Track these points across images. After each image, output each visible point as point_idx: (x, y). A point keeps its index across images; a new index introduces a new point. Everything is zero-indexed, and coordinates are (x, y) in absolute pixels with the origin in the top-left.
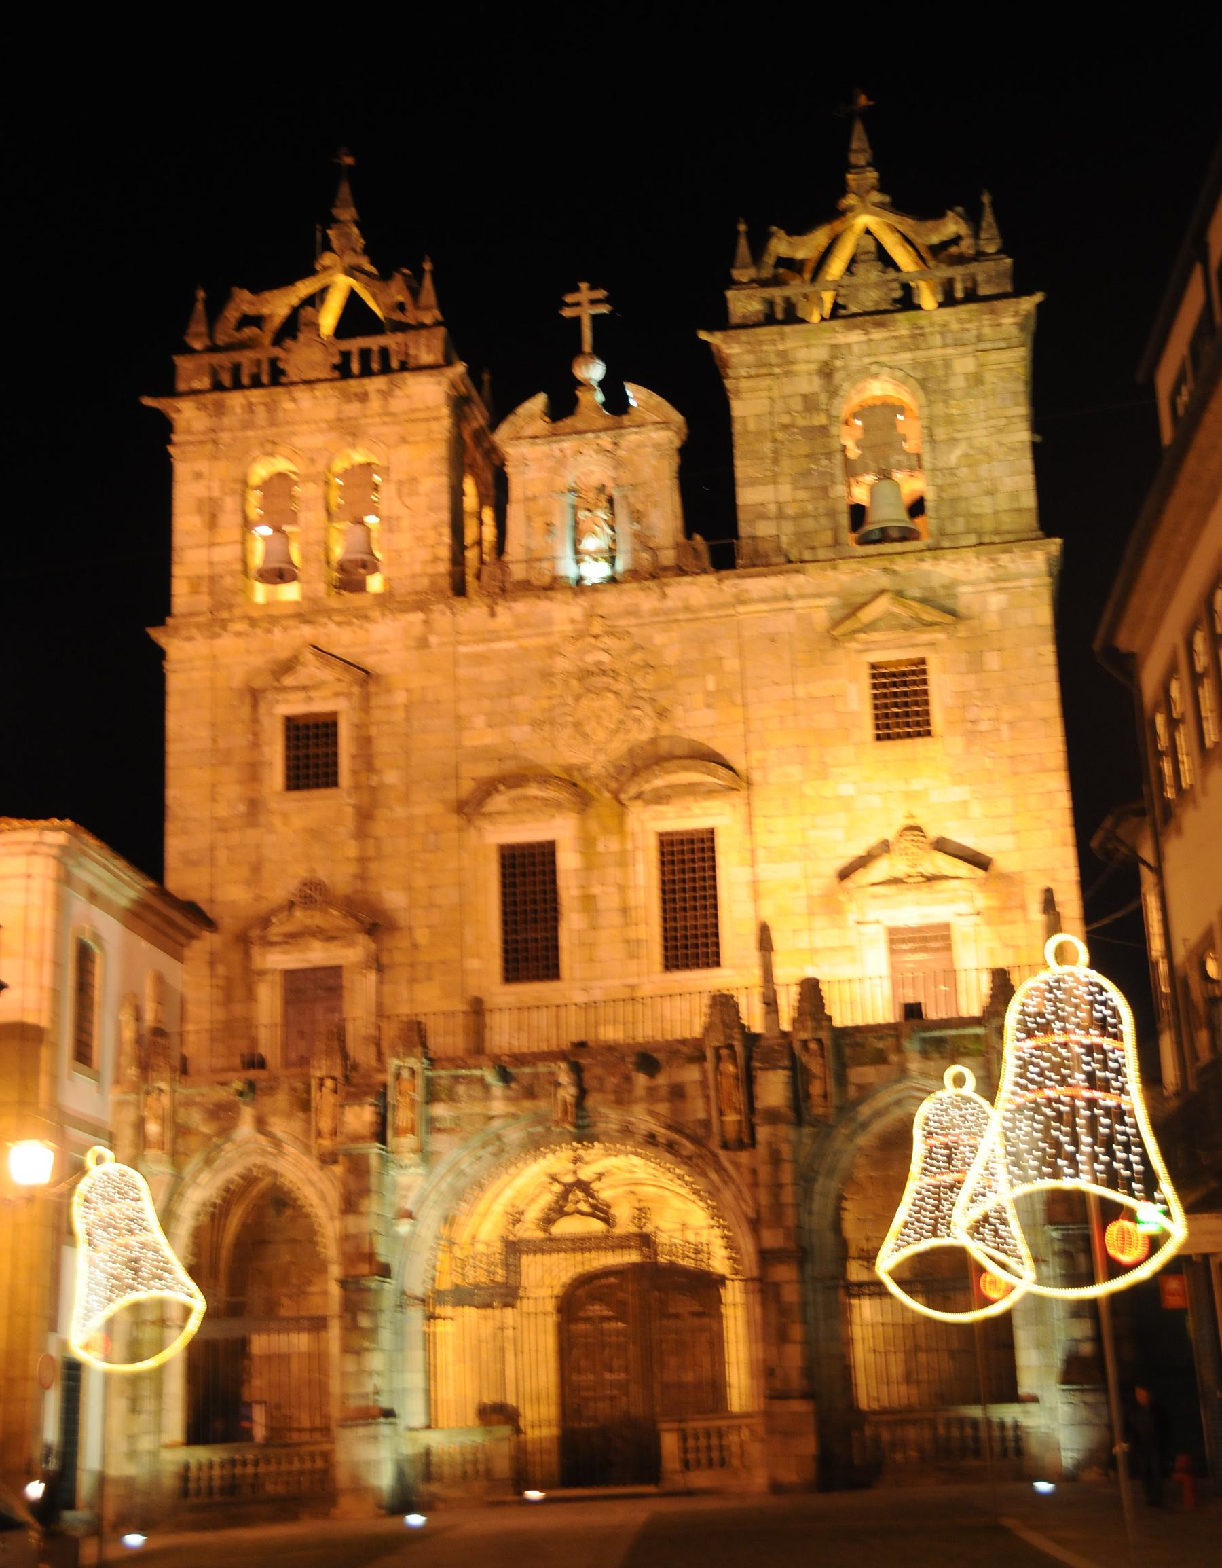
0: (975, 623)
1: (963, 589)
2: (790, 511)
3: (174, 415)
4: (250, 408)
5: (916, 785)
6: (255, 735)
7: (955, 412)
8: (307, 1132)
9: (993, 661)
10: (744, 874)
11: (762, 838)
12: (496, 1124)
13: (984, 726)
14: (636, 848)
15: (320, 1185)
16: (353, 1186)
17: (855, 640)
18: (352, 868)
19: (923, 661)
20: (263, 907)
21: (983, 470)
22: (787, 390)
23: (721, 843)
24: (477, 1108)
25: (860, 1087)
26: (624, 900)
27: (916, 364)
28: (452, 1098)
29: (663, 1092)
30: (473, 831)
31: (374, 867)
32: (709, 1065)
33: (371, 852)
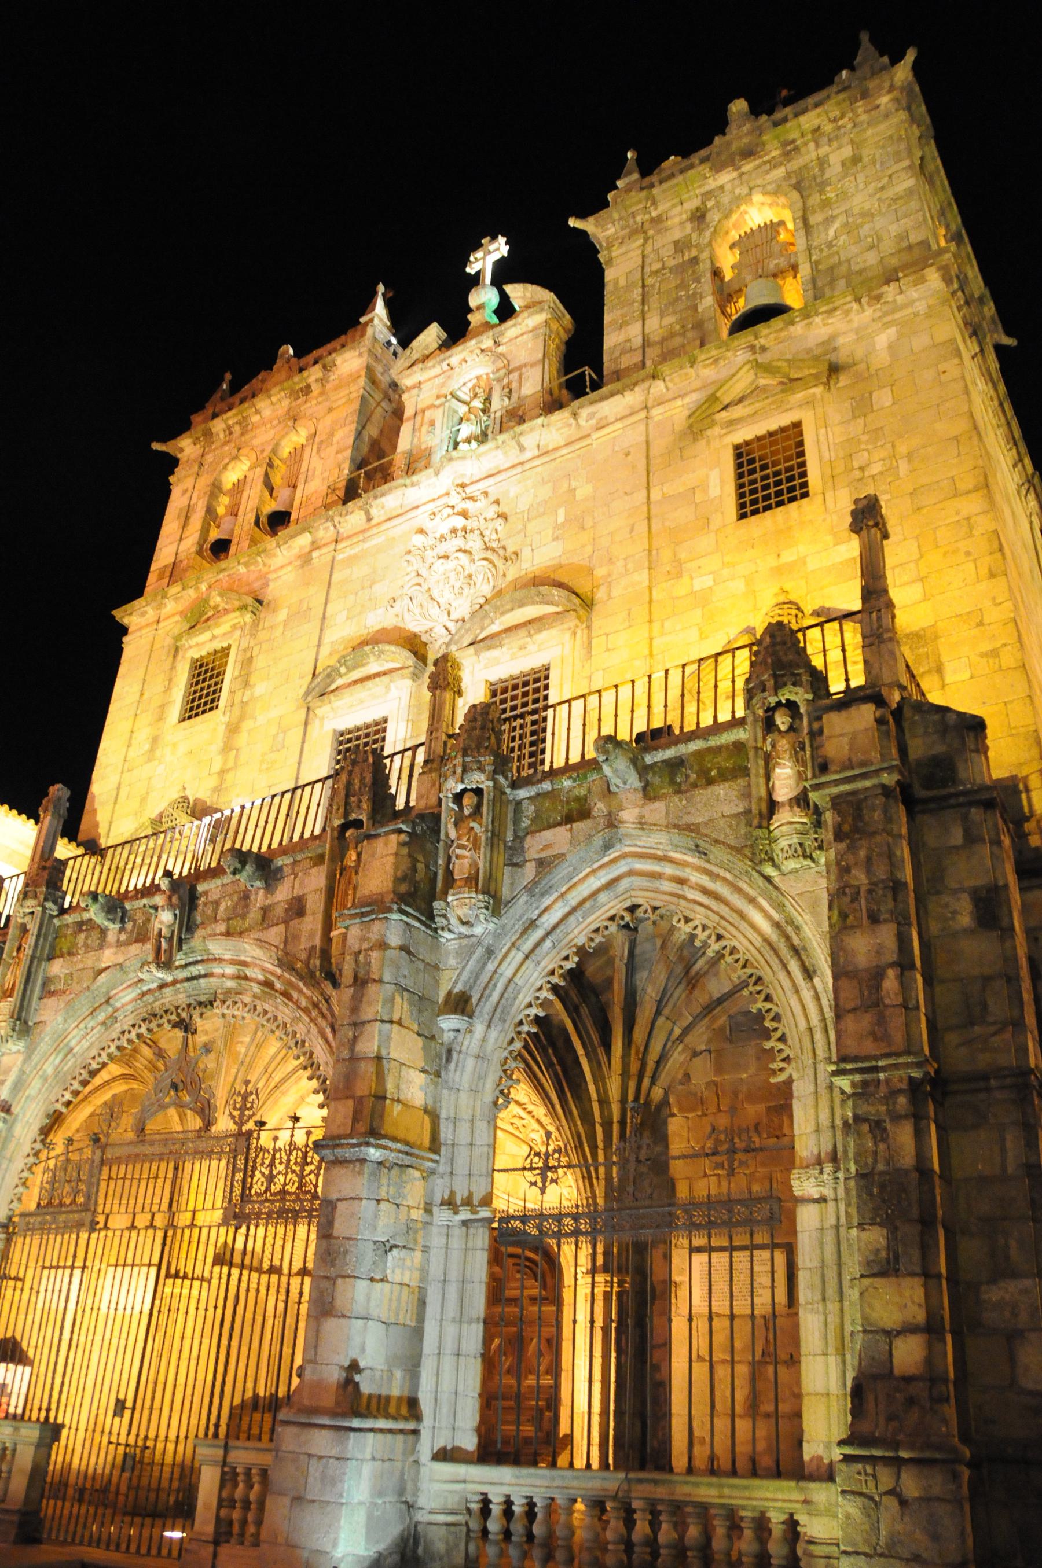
0: (863, 366)
1: (841, 341)
2: (655, 337)
3: (179, 456)
4: (229, 430)
5: (788, 556)
6: (170, 680)
7: (832, 195)
9: (883, 398)
12: (103, 978)
13: (875, 469)
17: (713, 423)
18: (213, 782)
19: (797, 425)
21: (865, 230)
22: (658, 244)
27: (789, 175)
29: (279, 912)
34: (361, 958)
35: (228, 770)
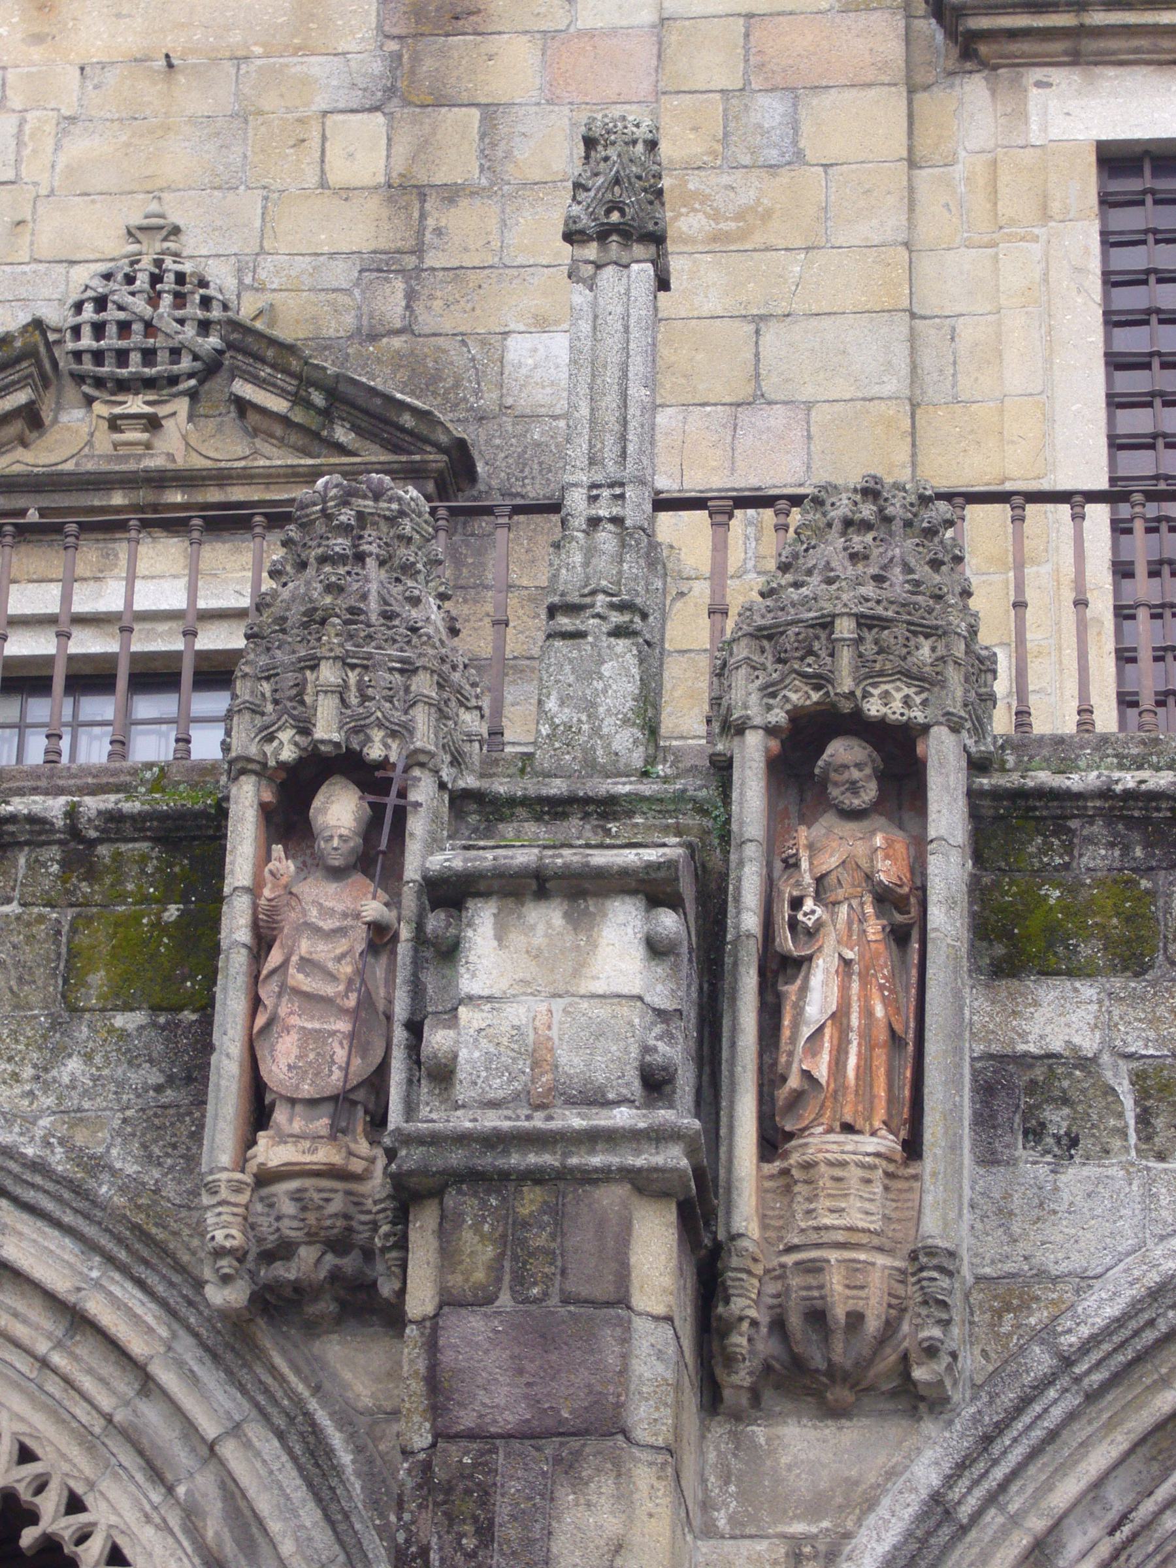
35: (452, 194)
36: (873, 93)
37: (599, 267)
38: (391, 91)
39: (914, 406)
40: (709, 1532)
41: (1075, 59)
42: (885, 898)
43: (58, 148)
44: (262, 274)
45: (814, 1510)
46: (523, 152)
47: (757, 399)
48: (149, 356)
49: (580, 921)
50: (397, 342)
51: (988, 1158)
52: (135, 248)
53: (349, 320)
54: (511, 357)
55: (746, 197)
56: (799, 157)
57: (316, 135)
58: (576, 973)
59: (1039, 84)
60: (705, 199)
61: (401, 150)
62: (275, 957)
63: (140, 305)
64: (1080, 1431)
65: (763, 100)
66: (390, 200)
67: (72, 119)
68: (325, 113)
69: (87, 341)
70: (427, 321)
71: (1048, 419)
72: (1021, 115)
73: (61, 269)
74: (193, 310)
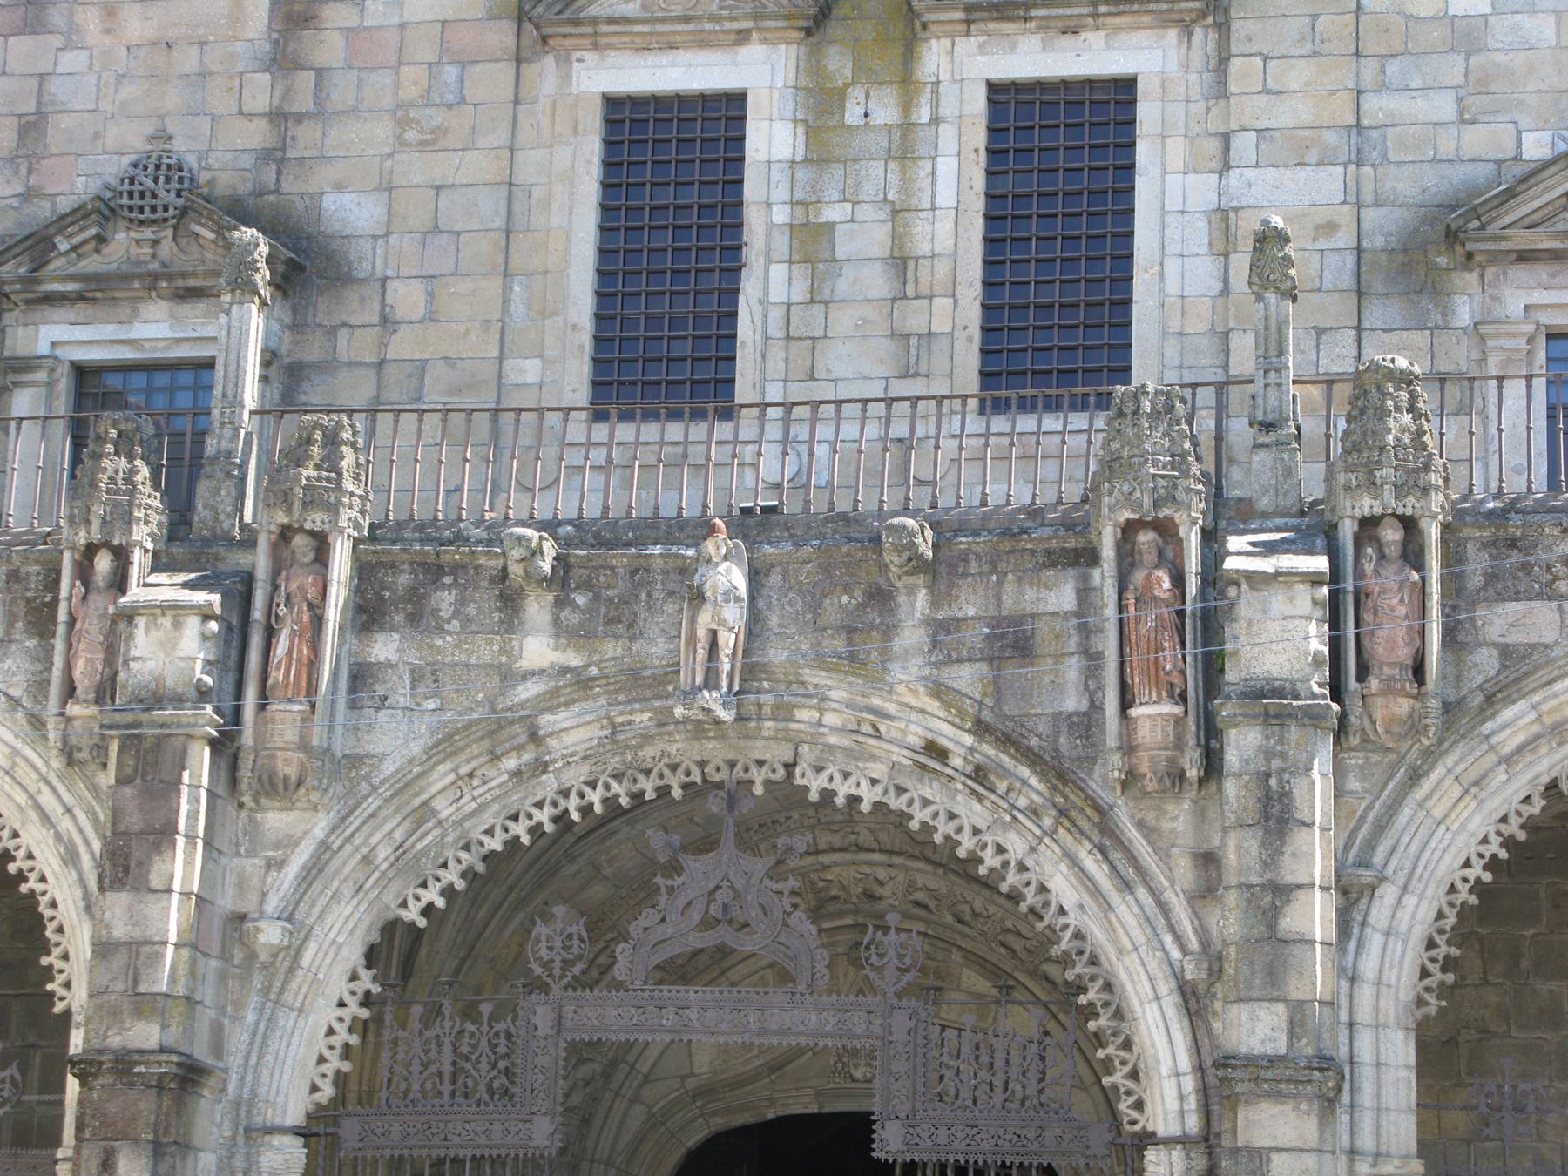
8: (39, 687)
10: (1202, 191)
11: (1249, 107)
14: (936, 121)
15: (66, 824)
16: (133, 821)
18: (257, 135)
20: (43, 211)
23: (1147, 113)
24: (485, 651)
25: (1507, 653)
26: (898, 239)
28: (419, 616)
29: (976, 636)
30: (549, 61)
31: (306, 137)
32: (1104, 577)
33: (303, 101)
34: (1273, 782)
35: (300, 118)
36: (499, 65)
37: (231, 304)
38: (274, 60)
39: (508, 232)
40: (238, 854)
41: (595, 46)
42: (311, 606)
43: (116, 91)
44: (210, 161)
45: (277, 846)
46: (335, 96)
47: (436, 230)
48: (154, 209)
49: (177, 625)
50: (272, 198)
51: (353, 705)
52: (149, 148)
53: (250, 185)
54: (324, 205)
55: (437, 121)
56: (463, 101)
57: (237, 83)
58: (174, 648)
59: (579, 60)
60: (418, 122)
61: (277, 94)
62: (78, 625)
63: (149, 183)
64: (384, 813)
65: (448, 68)
66: (271, 121)
67: (123, 76)
68: (241, 74)
69: (125, 201)
70: (286, 187)
71: (569, 240)
72: (568, 77)
73: (116, 157)
74: (175, 185)
